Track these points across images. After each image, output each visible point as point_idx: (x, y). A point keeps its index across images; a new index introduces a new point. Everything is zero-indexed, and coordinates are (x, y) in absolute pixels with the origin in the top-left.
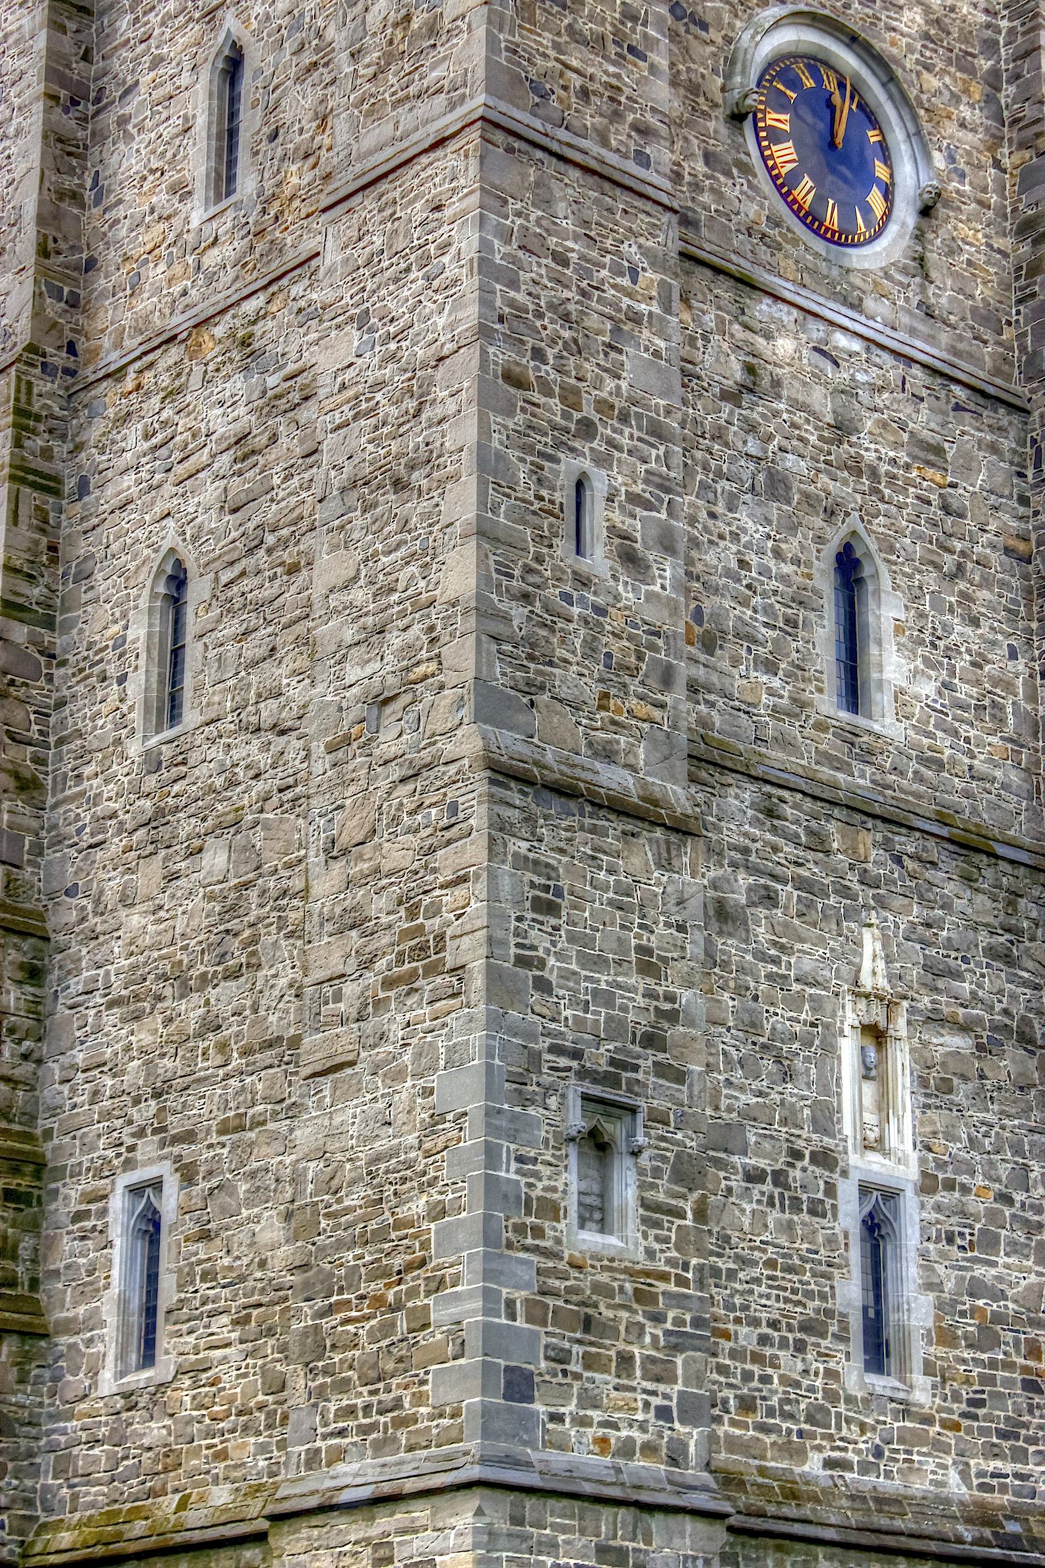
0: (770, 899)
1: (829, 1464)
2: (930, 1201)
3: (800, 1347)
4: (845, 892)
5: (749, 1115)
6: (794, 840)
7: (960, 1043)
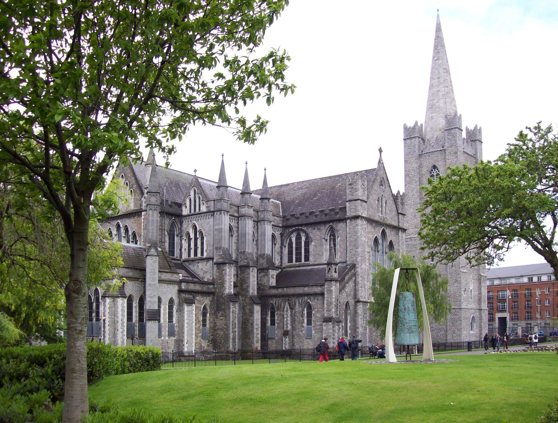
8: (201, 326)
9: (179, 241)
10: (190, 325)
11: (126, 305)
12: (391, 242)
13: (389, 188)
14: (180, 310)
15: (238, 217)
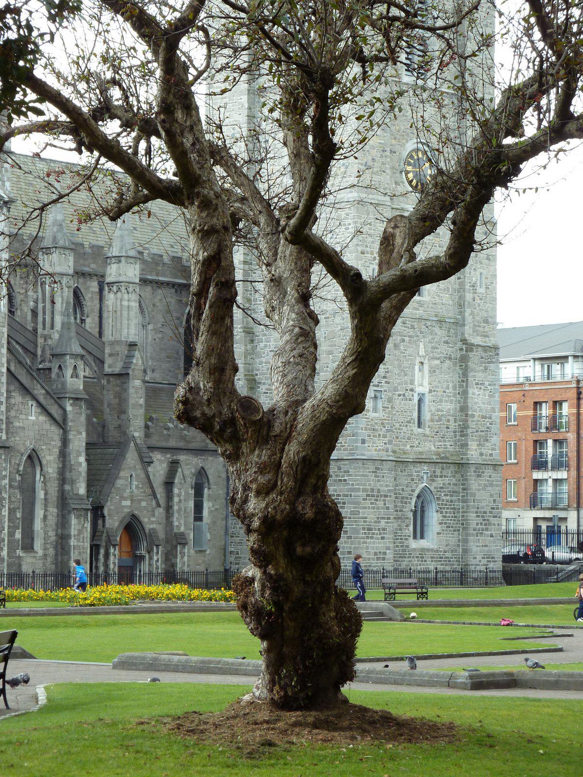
0: (403, 341)
1: (411, 447)
2: (430, 394)
3: (407, 426)
4: (417, 336)
5: (399, 384)
6: (408, 328)
7: (437, 362)
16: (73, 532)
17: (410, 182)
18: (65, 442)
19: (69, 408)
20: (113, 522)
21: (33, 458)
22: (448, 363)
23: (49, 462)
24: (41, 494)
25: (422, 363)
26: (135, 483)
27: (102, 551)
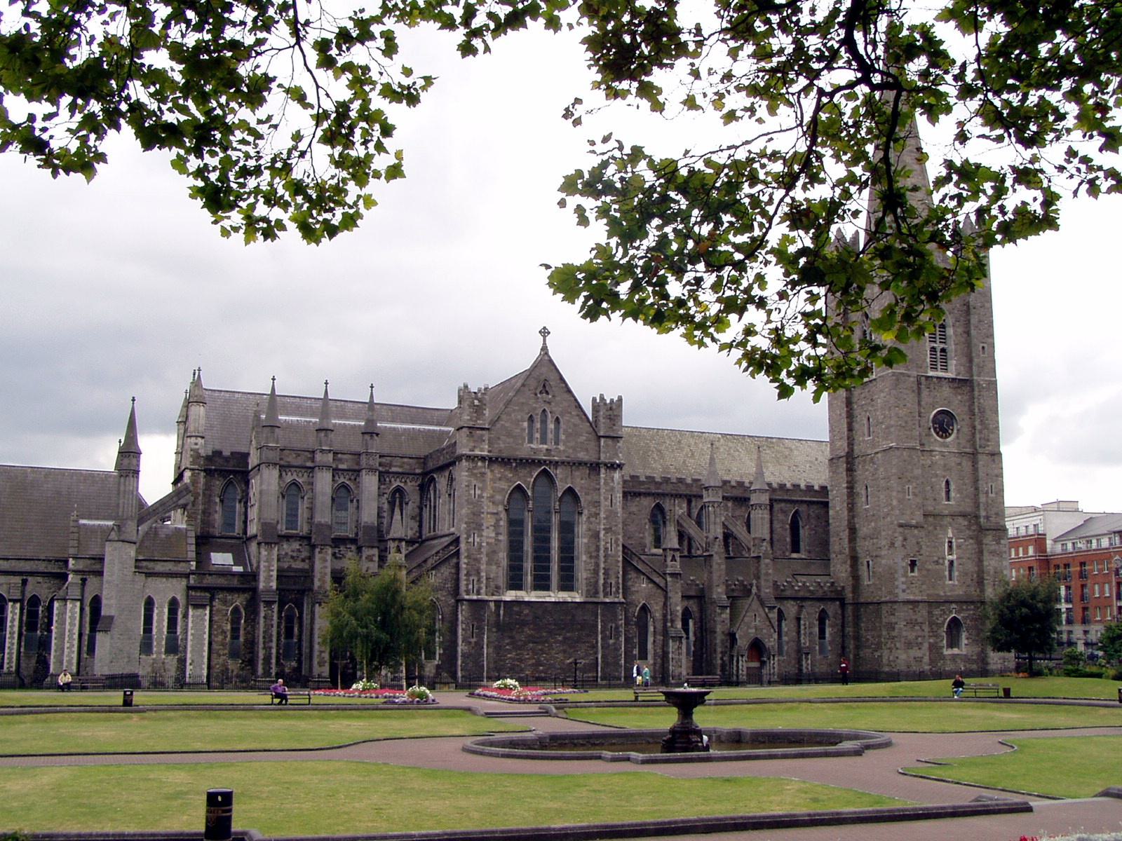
8: (228, 639)
9: (243, 510)
10: (198, 637)
11: (78, 610)
12: (570, 491)
13: (567, 396)
14: (186, 616)
15: (312, 468)
16: (671, 650)
17: (937, 434)
18: (666, 597)
19: (669, 579)
20: (743, 643)
21: (644, 609)
22: (971, 541)
23: (656, 610)
24: (651, 629)
25: (950, 542)
26: (758, 619)
27: (735, 659)
